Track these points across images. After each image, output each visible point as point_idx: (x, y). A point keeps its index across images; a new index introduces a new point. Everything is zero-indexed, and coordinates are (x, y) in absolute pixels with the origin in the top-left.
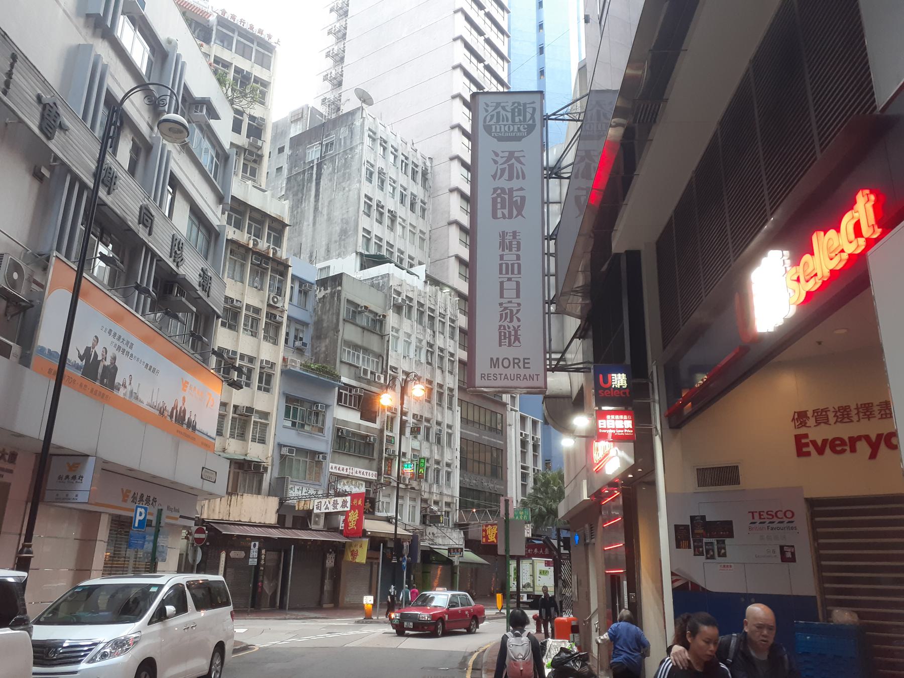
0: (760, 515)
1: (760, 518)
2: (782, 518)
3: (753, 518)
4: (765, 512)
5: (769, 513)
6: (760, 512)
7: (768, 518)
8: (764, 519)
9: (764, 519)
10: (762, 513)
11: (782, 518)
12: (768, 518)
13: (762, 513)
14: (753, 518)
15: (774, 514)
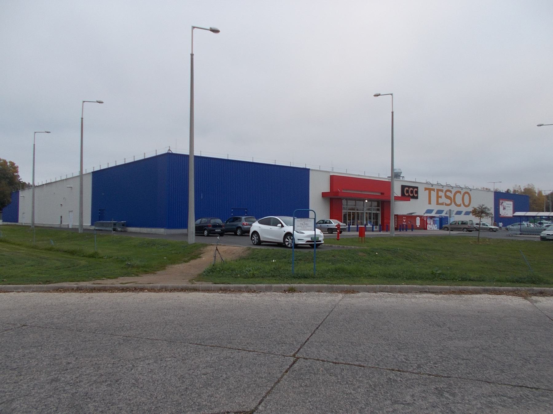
0: (438, 197)
1: (438, 203)
2: (460, 206)
3: (430, 203)
4: (444, 191)
5: (448, 194)
6: (438, 190)
7: (446, 205)
8: (442, 204)
9: (442, 204)
10: (440, 194)
11: (460, 206)
12: (446, 205)
13: (440, 194)
14: (430, 203)
15: (452, 196)
